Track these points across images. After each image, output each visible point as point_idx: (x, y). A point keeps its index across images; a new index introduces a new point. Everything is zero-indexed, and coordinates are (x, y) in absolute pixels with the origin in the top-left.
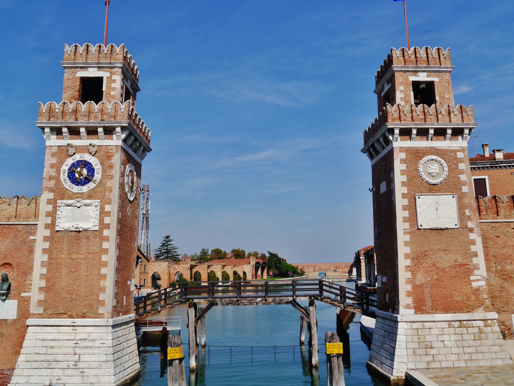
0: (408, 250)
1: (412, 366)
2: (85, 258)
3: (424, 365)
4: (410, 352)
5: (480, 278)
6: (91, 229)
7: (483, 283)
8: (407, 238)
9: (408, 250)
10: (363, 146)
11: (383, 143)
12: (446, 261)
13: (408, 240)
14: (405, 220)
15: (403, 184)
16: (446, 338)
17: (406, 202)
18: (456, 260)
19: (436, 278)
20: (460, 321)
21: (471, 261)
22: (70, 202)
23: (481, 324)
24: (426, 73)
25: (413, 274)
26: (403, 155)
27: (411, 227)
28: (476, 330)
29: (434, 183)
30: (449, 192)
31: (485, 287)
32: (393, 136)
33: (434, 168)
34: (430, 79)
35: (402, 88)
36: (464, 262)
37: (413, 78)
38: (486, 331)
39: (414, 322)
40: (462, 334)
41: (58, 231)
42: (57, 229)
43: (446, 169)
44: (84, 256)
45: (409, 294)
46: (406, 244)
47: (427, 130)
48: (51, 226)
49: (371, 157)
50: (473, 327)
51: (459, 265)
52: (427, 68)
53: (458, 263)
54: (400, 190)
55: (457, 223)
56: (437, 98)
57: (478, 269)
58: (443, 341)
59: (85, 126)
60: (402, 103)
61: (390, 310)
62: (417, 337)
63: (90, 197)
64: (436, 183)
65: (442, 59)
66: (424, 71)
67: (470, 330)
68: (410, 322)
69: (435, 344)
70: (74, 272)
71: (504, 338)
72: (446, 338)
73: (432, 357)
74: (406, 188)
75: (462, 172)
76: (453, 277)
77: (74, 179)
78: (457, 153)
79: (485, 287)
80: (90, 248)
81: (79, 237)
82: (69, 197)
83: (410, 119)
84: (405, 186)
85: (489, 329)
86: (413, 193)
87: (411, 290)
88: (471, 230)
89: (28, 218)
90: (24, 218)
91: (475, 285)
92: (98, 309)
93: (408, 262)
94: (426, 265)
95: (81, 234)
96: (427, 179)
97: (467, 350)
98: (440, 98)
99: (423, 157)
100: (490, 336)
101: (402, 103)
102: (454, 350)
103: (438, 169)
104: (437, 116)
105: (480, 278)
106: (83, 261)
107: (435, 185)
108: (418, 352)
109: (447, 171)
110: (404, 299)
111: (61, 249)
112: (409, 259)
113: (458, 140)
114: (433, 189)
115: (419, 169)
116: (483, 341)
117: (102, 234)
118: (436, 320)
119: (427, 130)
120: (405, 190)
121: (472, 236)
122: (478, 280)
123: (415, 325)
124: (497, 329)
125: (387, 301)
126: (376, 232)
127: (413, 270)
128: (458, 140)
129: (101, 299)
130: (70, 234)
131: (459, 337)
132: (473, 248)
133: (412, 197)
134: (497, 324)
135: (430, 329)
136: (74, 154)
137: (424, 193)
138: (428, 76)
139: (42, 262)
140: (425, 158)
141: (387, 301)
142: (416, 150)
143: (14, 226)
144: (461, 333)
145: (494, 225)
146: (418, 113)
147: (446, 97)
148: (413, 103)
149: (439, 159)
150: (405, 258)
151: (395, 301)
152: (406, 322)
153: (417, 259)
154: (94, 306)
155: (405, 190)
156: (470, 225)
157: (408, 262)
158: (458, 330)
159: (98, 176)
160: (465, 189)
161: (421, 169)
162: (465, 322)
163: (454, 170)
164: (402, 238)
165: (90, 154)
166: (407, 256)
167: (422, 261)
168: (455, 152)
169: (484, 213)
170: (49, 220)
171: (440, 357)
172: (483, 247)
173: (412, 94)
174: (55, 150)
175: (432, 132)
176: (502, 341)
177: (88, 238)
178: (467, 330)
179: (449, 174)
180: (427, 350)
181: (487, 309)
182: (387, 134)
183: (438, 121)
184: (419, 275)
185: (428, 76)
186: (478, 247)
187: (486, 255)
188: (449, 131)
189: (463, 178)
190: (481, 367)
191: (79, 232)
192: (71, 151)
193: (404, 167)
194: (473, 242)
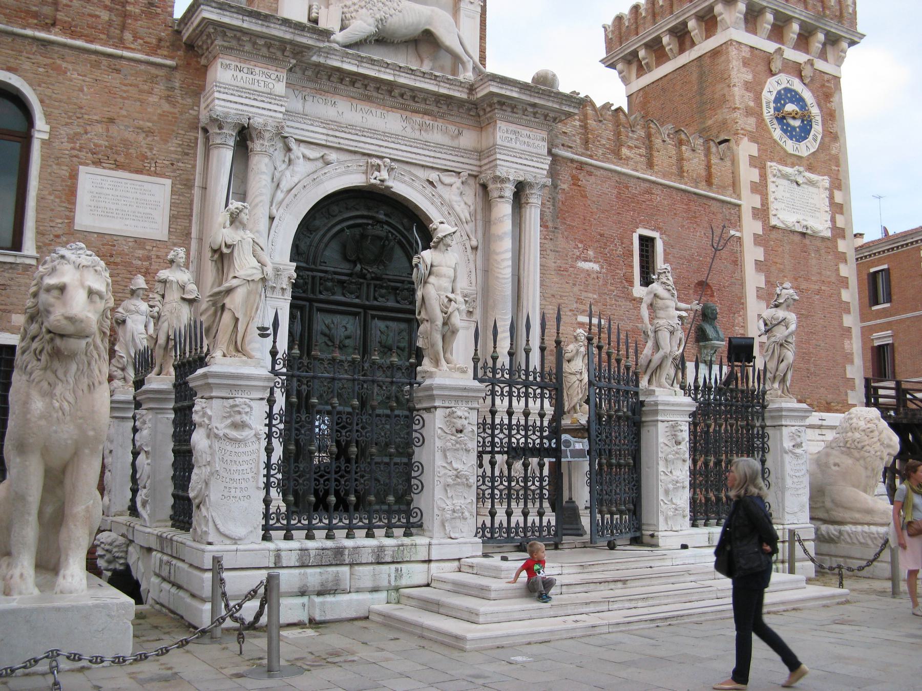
2: (818, 292)
6: (822, 234)
22: (788, 170)
41: (774, 227)
42: (774, 222)
44: (817, 287)
48: (762, 213)
59: (803, 21)
63: (811, 168)
70: (807, 317)
77: (784, 124)
80: (824, 272)
81: (805, 246)
82: (781, 159)
89: (722, 188)
90: (719, 187)
92: (846, 395)
95: (807, 241)
106: (817, 297)
111: (782, 267)
117: (836, 247)
129: (849, 376)
130: (791, 235)
136: (779, 72)
139: (758, 289)
143: (705, 201)
154: (841, 388)
159: (817, 128)
165: (802, 81)
170: (756, 201)
174: (746, 53)
177: (818, 250)
191: (804, 234)
192: (776, 65)
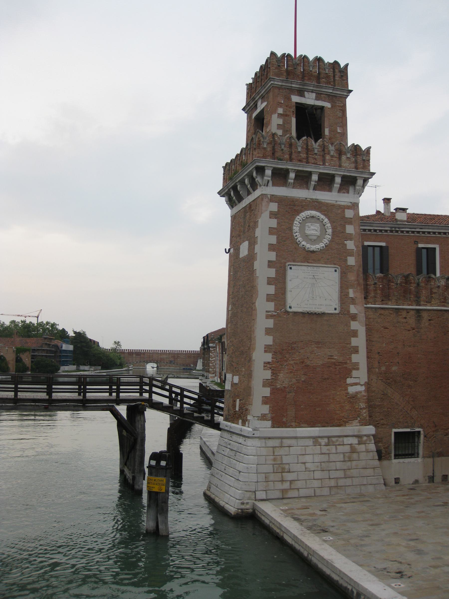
0: (269, 340)
1: (261, 495)
3: (278, 494)
4: (262, 477)
5: (358, 382)
7: (363, 388)
8: (270, 323)
9: (269, 340)
10: (221, 187)
11: (249, 186)
13: (271, 326)
14: (269, 298)
16: (308, 458)
17: (272, 273)
18: (331, 357)
19: (303, 379)
20: (329, 437)
21: (350, 359)
23: (355, 441)
24: (314, 95)
25: (273, 374)
26: (274, 207)
27: (276, 309)
28: (347, 449)
29: (312, 249)
30: (331, 264)
31: (364, 393)
32: (263, 178)
33: (313, 229)
34: (319, 103)
35: (280, 111)
36: (341, 359)
37: (296, 99)
38: (359, 451)
39: (269, 438)
40: (329, 454)
43: (330, 231)
45: (265, 401)
46: (268, 331)
47: (310, 173)
49: (231, 203)
50: (343, 445)
51: (334, 364)
52: (317, 87)
53: (333, 360)
55: (337, 307)
56: (327, 132)
57: (358, 369)
58: (305, 463)
60: (280, 132)
61: (240, 421)
62: (272, 457)
64: (315, 250)
65: (337, 78)
66: (312, 91)
67: (340, 449)
68: (265, 438)
69: (294, 467)
71: (380, 458)
72: (308, 458)
73: (288, 483)
74: (274, 253)
75: (349, 237)
76: (325, 379)
78: (346, 210)
79: (364, 393)
83: (287, 156)
84: (274, 250)
85: (362, 448)
86: (283, 261)
87: (269, 395)
88: (354, 317)
91: (352, 390)
93: (269, 357)
94: (292, 362)
96: (304, 243)
97: (334, 474)
98: (330, 131)
99: (302, 211)
100: (363, 456)
101: (280, 132)
102: (318, 475)
103: (319, 230)
104: (324, 156)
105: (358, 382)
107: (313, 252)
108: (272, 477)
109: (331, 234)
110: (258, 407)
112: (270, 352)
113: (348, 192)
114: (310, 257)
115: (294, 228)
116: (354, 463)
118: (299, 435)
119: (310, 173)
120: (272, 256)
121: (354, 325)
122: (356, 384)
123: (271, 443)
124: (372, 447)
125: (237, 409)
126: (230, 312)
128: (348, 192)
131: (325, 458)
132: (354, 342)
133: (281, 267)
134: (373, 442)
135: (289, 447)
137: (298, 262)
138: (317, 99)
140: (303, 214)
141: (237, 409)
142: (293, 201)
144: (328, 452)
145: (382, 312)
146: (300, 149)
147: (339, 131)
148: (294, 134)
149: (322, 217)
150: (265, 351)
151: (247, 410)
152: (259, 438)
153: (281, 353)
155: (272, 256)
156: (353, 309)
157: (269, 357)
158: (325, 449)
161: (296, 228)
162: (334, 439)
164: (262, 323)
166: (267, 349)
167: (287, 356)
168: (343, 208)
169: (372, 294)
171: (299, 484)
172: (367, 340)
173: (294, 120)
175: (315, 177)
176: (377, 463)
178: (336, 449)
179: (332, 238)
180: (284, 474)
181: (364, 423)
182: (254, 174)
183: (324, 164)
184: (281, 375)
185: (317, 99)
186: (360, 341)
187: (369, 351)
188: (338, 180)
189: (350, 245)
190: (348, 495)
193: (274, 223)
194: (355, 334)
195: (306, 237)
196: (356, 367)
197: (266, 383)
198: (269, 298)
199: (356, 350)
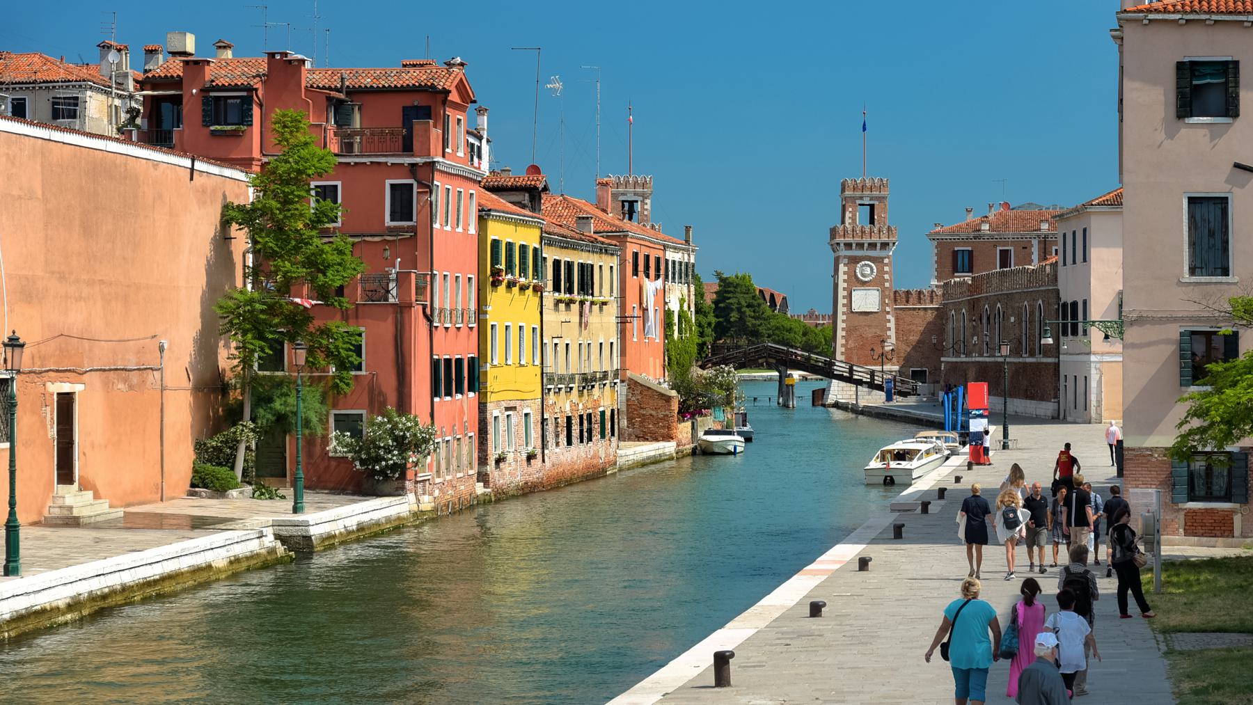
0: (844, 325)
9: (844, 325)
12: (869, 333)
14: (844, 305)
15: (845, 281)
33: (868, 271)
54: (842, 285)
120: (845, 285)
121: (888, 317)
127: (846, 338)
153: (849, 331)
155: (845, 285)
156: (888, 309)
160: (887, 285)
161: (858, 271)
163: (881, 272)
186: (892, 325)
189: (887, 277)
195: (863, 275)
196: (889, 337)
197: (843, 345)
198: (844, 305)
199: (889, 329)
